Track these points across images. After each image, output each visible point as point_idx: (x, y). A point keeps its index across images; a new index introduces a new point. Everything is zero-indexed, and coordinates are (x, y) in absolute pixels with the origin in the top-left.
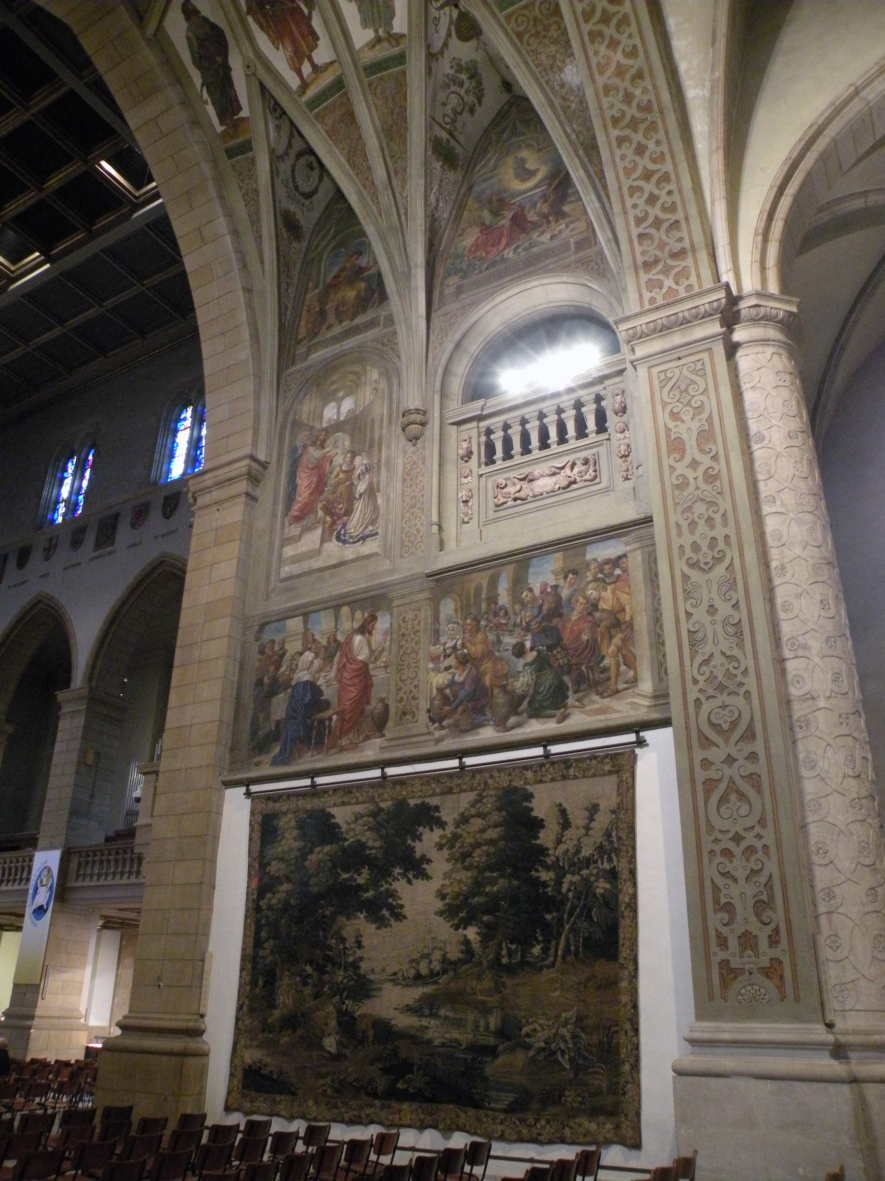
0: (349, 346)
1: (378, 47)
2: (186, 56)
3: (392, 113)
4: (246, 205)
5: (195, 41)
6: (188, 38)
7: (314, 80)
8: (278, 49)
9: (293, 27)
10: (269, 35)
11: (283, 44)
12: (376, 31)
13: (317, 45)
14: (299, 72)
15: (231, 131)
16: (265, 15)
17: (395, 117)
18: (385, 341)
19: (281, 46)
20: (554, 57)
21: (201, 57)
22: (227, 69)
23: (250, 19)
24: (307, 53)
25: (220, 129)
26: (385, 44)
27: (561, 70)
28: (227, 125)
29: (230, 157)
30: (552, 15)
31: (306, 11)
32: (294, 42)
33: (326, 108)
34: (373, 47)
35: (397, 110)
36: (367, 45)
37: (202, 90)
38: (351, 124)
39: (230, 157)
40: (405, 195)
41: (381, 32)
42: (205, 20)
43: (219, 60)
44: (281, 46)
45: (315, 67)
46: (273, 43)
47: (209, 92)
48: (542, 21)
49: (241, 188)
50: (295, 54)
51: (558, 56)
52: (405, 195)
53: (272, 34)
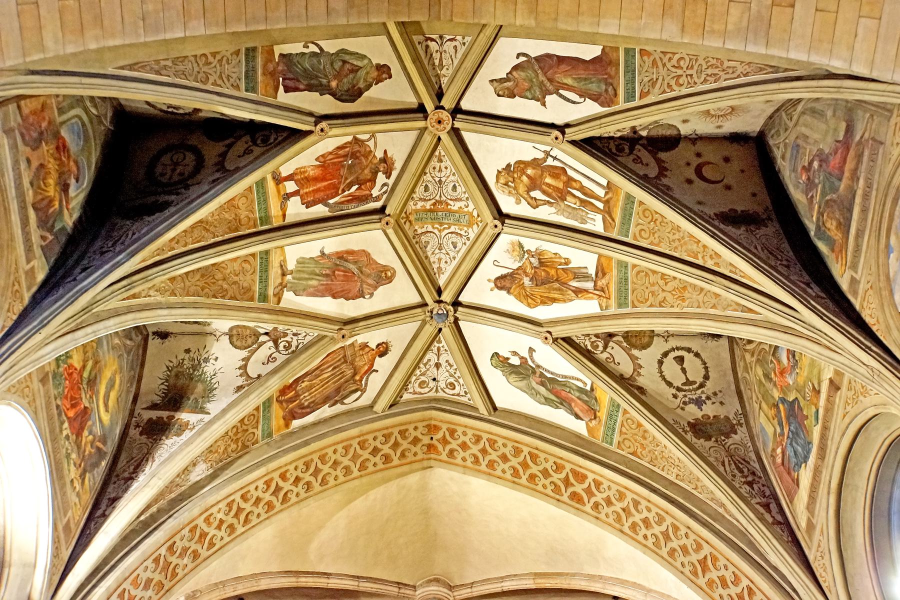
0: (13, 217)
1: (280, 272)
2: (352, 44)
3: (224, 279)
4: (195, 56)
5: (359, 63)
6: (364, 57)
7: (279, 191)
8: (317, 159)
9: (326, 183)
10: (331, 153)
11: (318, 166)
12: (292, 272)
13: (303, 204)
14: (290, 178)
15: (271, 67)
16: (346, 156)
17: (220, 282)
18: (17, 287)
19: (318, 163)
20: (217, 451)
21: (344, 62)
22: (323, 90)
23: (350, 138)
24: (301, 192)
25: (278, 50)
26: (279, 281)
27: (205, 462)
28: (278, 64)
29: (247, 49)
30: (243, 444)
31: (331, 201)
32: (316, 179)
33: (252, 201)
34: (281, 266)
35: (225, 286)
36: (285, 261)
37: (317, 45)
38: (229, 228)
39: (247, 49)
40: (152, 293)
41: (289, 277)
42: (369, 87)
43: (334, 84)
44: (318, 163)
45: (288, 196)
46: (323, 156)
47: (314, 54)
48: (243, 436)
49: (214, 55)
50: (306, 178)
51: (216, 455)
52: (152, 293)
53: (330, 157)
